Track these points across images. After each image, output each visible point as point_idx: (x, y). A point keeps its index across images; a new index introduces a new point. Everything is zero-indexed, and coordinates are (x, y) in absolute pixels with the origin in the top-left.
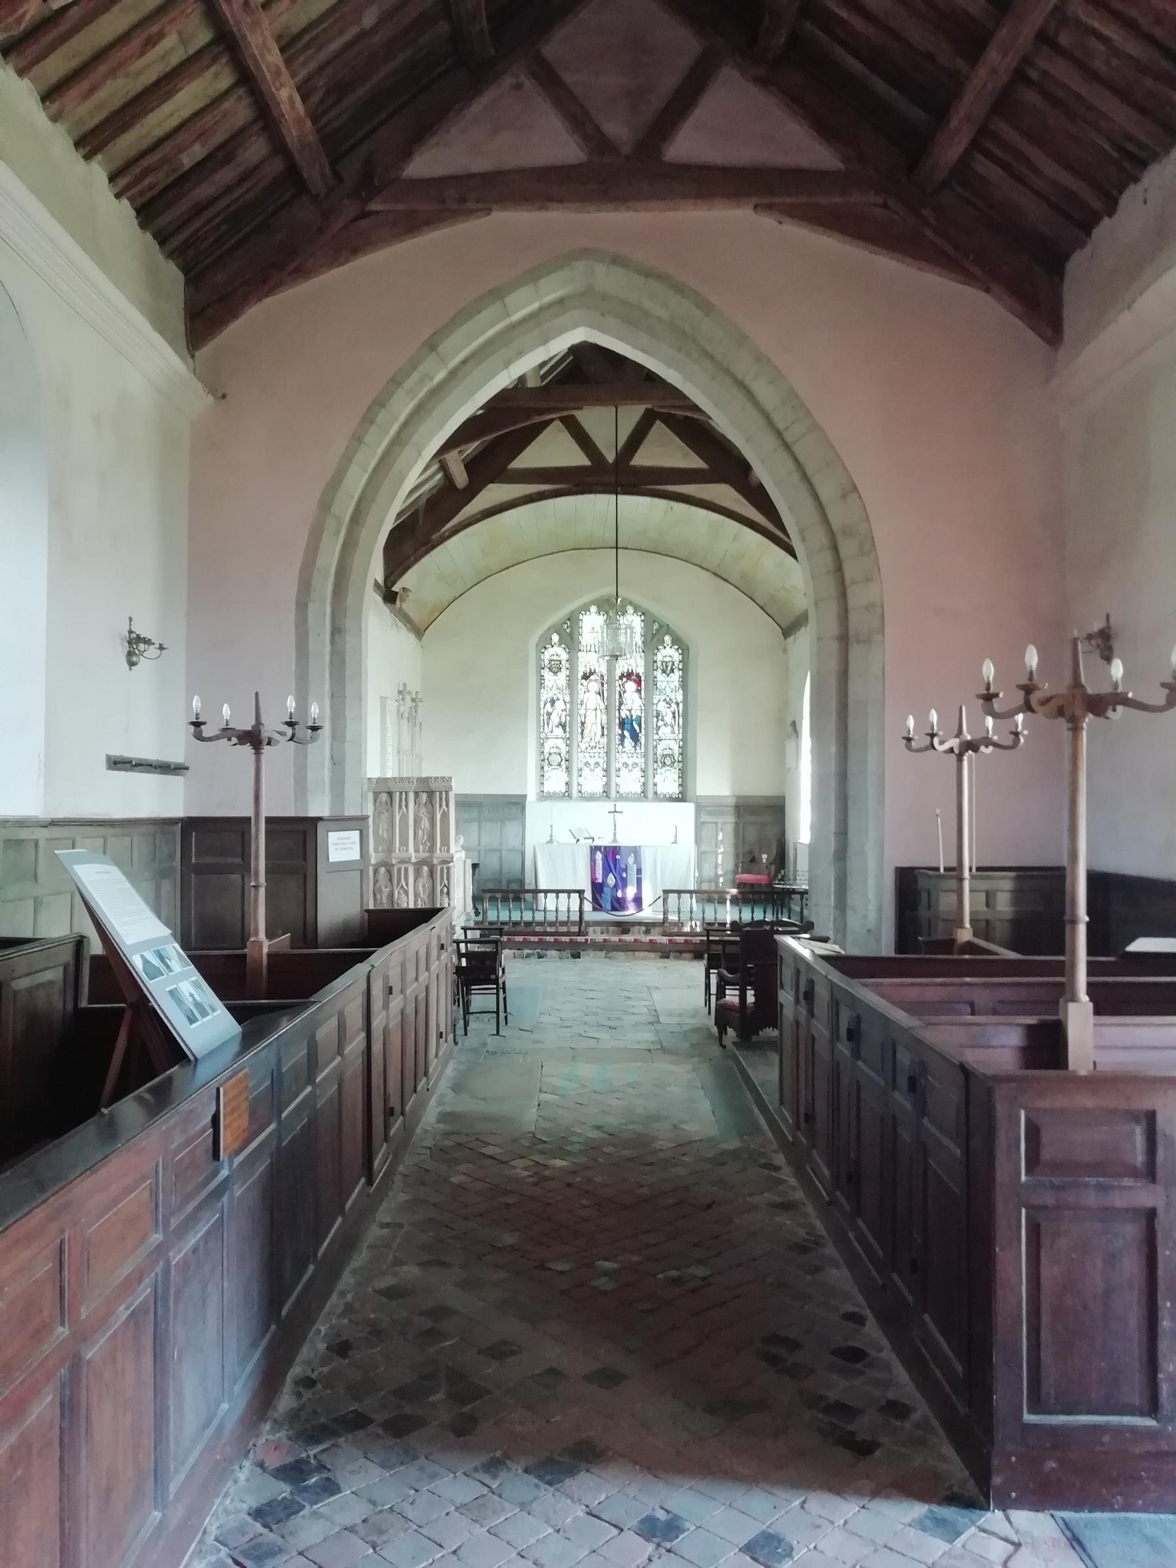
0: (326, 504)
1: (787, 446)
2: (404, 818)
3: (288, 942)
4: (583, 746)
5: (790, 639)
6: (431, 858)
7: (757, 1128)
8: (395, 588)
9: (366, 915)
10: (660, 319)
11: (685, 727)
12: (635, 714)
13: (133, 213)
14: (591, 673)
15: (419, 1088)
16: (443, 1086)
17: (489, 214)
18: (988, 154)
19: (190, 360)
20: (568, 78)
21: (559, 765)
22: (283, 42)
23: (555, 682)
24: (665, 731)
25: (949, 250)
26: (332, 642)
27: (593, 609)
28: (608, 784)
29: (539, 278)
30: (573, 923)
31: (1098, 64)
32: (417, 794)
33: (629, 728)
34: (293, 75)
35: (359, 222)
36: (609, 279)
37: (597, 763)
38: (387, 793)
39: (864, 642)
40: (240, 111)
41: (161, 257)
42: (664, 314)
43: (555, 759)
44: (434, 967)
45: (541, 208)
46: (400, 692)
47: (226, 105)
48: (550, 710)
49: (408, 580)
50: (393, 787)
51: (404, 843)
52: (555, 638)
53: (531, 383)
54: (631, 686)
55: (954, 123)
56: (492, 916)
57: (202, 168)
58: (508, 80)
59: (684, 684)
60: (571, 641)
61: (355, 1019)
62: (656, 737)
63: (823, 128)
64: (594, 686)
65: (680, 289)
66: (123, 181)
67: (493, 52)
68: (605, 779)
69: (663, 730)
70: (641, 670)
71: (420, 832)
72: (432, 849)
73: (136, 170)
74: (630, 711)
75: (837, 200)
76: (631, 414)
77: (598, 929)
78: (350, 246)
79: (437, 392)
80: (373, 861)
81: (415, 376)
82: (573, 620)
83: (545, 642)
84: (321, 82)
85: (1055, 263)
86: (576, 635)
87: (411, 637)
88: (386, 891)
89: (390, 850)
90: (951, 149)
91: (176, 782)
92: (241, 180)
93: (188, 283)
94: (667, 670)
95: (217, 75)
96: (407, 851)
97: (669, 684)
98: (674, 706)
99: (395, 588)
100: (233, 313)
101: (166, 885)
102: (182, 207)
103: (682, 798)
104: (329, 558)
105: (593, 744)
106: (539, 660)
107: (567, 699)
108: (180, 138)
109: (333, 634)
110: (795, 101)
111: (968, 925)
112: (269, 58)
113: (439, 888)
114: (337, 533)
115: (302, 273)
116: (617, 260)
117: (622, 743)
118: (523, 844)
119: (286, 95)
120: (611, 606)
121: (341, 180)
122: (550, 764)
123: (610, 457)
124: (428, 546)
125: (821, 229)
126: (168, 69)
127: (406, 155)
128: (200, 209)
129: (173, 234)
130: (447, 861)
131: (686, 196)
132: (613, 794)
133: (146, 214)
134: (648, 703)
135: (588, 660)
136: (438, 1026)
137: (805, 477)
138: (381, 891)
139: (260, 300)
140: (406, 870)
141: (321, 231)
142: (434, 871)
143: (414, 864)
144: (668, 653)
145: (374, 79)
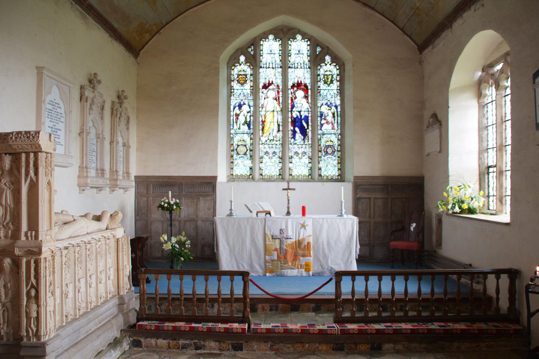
4: (263, 139)
6: (12, 246)
12: (303, 114)
14: (270, 84)
21: (245, 154)
23: (241, 92)
27: (271, 37)
28: (282, 169)
33: (299, 124)
37: (274, 152)
43: (242, 150)
48: (238, 112)
52: (242, 58)
54: (300, 94)
59: (341, 91)
60: (254, 61)
62: (320, 132)
64: (272, 94)
68: (281, 165)
69: (325, 127)
70: (308, 82)
72: (16, 235)
74: (300, 112)
82: (255, 43)
83: (233, 61)
86: (258, 56)
94: (328, 81)
97: (330, 93)
98: (333, 108)
103: (341, 178)
106: (229, 75)
107: (252, 103)
117: (294, 137)
118: (214, 215)
122: (238, 154)
132: (287, 176)
134: (314, 105)
135: (267, 75)
144: (329, 68)
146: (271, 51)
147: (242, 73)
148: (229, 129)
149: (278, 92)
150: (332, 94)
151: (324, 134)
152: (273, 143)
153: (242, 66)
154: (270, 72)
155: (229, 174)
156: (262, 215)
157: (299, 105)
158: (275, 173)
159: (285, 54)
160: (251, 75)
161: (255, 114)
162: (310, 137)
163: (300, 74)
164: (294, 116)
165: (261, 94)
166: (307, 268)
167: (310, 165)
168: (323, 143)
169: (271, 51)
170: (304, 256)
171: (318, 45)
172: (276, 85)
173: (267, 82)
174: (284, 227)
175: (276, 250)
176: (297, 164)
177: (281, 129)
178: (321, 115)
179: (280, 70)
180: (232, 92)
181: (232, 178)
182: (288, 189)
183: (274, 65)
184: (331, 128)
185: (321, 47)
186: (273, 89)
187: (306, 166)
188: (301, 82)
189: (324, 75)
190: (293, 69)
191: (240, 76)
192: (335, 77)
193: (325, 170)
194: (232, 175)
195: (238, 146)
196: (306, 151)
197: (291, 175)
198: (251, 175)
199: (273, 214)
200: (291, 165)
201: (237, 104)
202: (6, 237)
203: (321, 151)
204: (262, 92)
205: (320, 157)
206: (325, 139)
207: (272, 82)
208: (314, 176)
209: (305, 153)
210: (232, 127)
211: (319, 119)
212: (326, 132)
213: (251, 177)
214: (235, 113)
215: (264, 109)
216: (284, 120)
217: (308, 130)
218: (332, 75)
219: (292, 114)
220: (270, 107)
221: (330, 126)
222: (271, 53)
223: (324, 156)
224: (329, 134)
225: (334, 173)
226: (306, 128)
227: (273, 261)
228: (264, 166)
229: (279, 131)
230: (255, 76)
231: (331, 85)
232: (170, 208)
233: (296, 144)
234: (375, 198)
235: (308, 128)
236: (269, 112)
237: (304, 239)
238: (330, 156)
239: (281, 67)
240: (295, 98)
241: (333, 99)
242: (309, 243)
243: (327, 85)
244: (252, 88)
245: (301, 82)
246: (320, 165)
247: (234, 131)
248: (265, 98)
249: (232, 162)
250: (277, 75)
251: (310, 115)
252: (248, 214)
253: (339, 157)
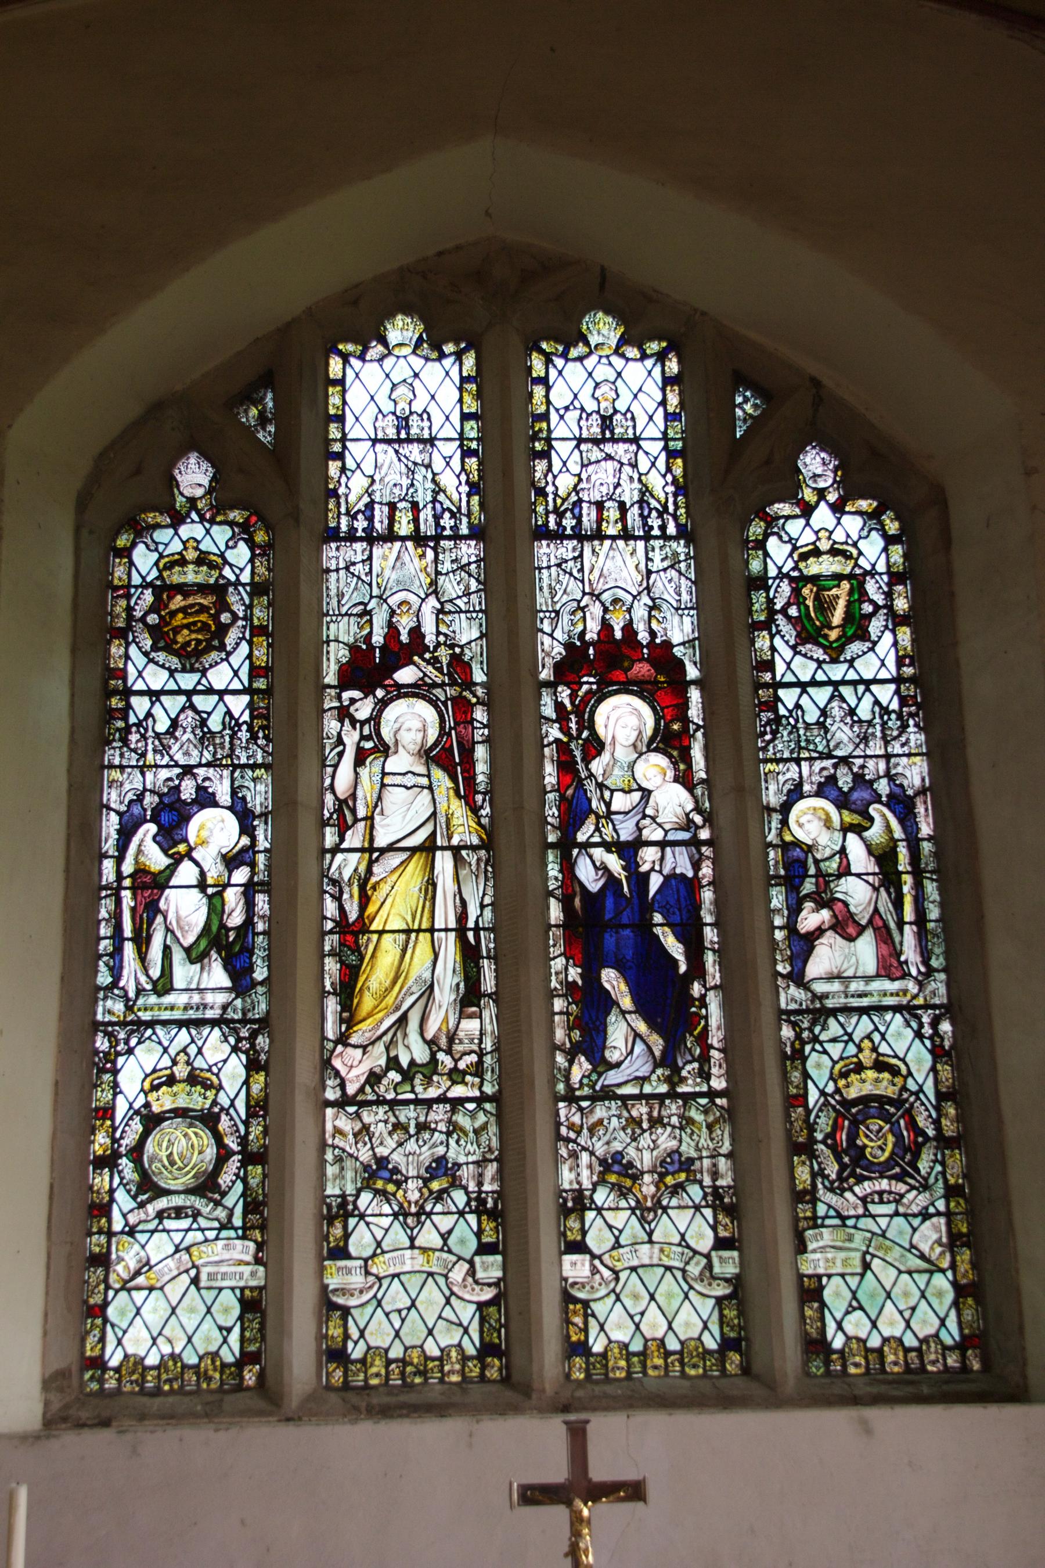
4: (354, 1066)
11: (961, 940)
21: (207, 1186)
27: (401, 330)
37: (440, 1167)
48: (156, 859)
52: (194, 476)
54: (623, 718)
59: (931, 690)
60: (284, 490)
62: (791, 996)
64: (411, 721)
68: (491, 1268)
69: (825, 958)
74: (628, 850)
83: (124, 497)
98: (883, 822)
105: (414, 1050)
107: (259, 794)
117: (591, 1043)
122: (148, 1187)
134: (730, 803)
144: (827, 531)
146: (403, 422)
147: (191, 575)
149: (463, 708)
150: (864, 711)
151: (821, 1013)
152: (433, 1093)
153: (192, 530)
154: (399, 567)
155: (67, 1359)
157: (620, 802)
158: (448, 1337)
159: (506, 436)
160: (257, 589)
162: (715, 1038)
163: (629, 581)
165: (332, 725)
167: (728, 1264)
169: (403, 422)
171: (740, 380)
172: (444, 654)
173: (378, 639)
176: (626, 1258)
177: (489, 983)
178: (792, 879)
179: (469, 551)
180: (110, 715)
183: (426, 515)
184: (869, 963)
185: (759, 391)
186: (419, 690)
187: (695, 1269)
188: (629, 629)
189: (798, 581)
190: (567, 549)
191: (178, 602)
193: (856, 1305)
194: (99, 1363)
195: (152, 1121)
196: (688, 1150)
197: (582, 1348)
198: (246, 1358)
200: (575, 1268)
201: (149, 800)
203: (807, 1149)
204: (344, 714)
205: (810, 1196)
206: (835, 1050)
207: (416, 633)
208: (765, 1355)
209: (687, 1165)
210: (104, 978)
211: (778, 898)
213: (242, 1387)
214: (128, 868)
215: (354, 838)
216: (513, 905)
217: (696, 989)
218: (858, 581)
219: (568, 867)
220: (401, 817)
221: (865, 952)
222: (404, 433)
223: (839, 1187)
225: (926, 1323)
226: (683, 968)
228: (357, 1280)
229: (470, 997)
230: (289, 599)
231: (855, 648)
233: (607, 1094)
235: (697, 970)
236: (395, 860)
238: (884, 1184)
239: (477, 533)
240: (595, 746)
241: (876, 747)
243: (819, 654)
244: (261, 684)
245: (629, 629)
246: (813, 1263)
247: (119, 1007)
248: (361, 758)
249: (102, 1260)
250: (451, 587)
251: (706, 870)
253: (951, 1192)
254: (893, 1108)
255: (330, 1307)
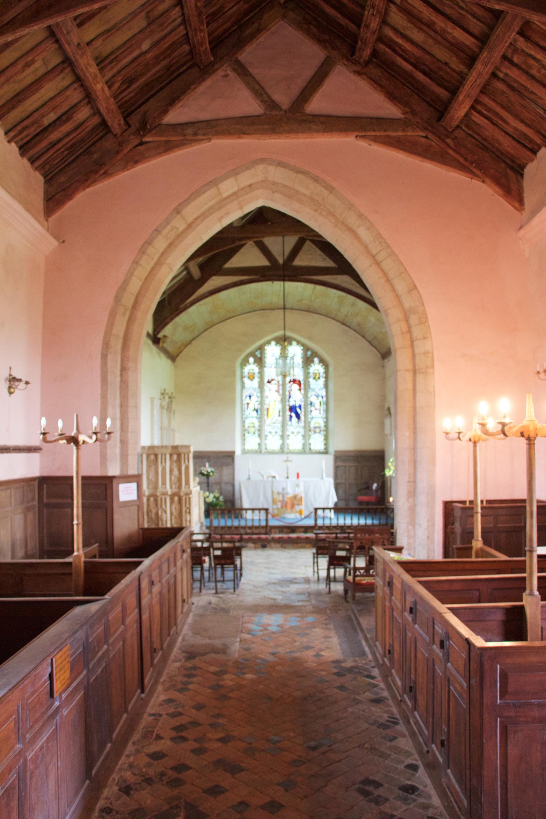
0: (118, 299)
1: (378, 264)
2: (164, 469)
3: (97, 550)
5: (386, 360)
6: (180, 491)
7: (363, 654)
8: (160, 336)
9: (141, 531)
10: (305, 195)
13: (17, 149)
15: (172, 633)
16: (186, 630)
17: (210, 142)
18: (479, 112)
19: (46, 223)
20: (252, 71)
22: (99, 60)
23: (251, 385)
24: (315, 413)
25: (462, 160)
26: (121, 375)
27: (273, 343)
28: (283, 445)
29: (237, 174)
30: (263, 527)
31: (534, 72)
32: (171, 455)
34: (103, 77)
35: (139, 147)
36: (276, 174)
37: (276, 432)
38: (153, 454)
39: (423, 373)
40: (76, 96)
41: (32, 170)
42: (307, 193)
43: (252, 430)
44: (179, 563)
45: (239, 138)
46: (162, 394)
47: (68, 93)
49: (167, 331)
50: (157, 451)
51: (164, 483)
52: (251, 360)
53: (236, 225)
54: (295, 387)
55: (461, 98)
56: (215, 523)
57: (54, 124)
58: (221, 73)
59: (326, 386)
60: (260, 361)
61: (132, 600)
63: (391, 96)
64: (273, 386)
65: (316, 179)
66: (12, 134)
67: (212, 59)
71: (173, 478)
72: (180, 487)
73: (19, 128)
75: (400, 134)
76: (291, 241)
77: (277, 530)
78: (134, 160)
79: (181, 236)
80: (147, 493)
81: (169, 227)
82: (261, 348)
83: (245, 362)
84: (120, 78)
85: (519, 170)
86: (263, 358)
87: (169, 362)
88: (154, 511)
89: (156, 487)
90: (460, 110)
91: (35, 456)
92: (75, 129)
93: (46, 182)
95: (63, 78)
96: (165, 488)
97: (317, 386)
98: (320, 399)
99: (160, 336)
100: (69, 197)
101: (30, 516)
102: (44, 144)
103: (326, 452)
104: (119, 329)
105: (274, 421)
106: (242, 373)
107: (259, 395)
108: (42, 111)
109: (121, 371)
110: (376, 83)
111: (480, 539)
112: (91, 70)
113: (184, 509)
114: (124, 314)
115: (107, 174)
116: (281, 164)
119: (99, 87)
120: (284, 341)
121: (129, 126)
123: (281, 261)
124: (177, 311)
125: (392, 149)
126: (37, 77)
127: (165, 112)
128: (53, 145)
129: (38, 158)
130: (188, 494)
131: (318, 131)
133: (23, 149)
134: (306, 396)
135: (270, 372)
136: (182, 596)
137: (388, 280)
138: (151, 511)
139: (84, 189)
140: (165, 499)
141: (118, 153)
142: (181, 500)
143: (170, 496)
144: (317, 368)
145: (149, 75)
147: (251, 371)
148: (242, 415)
151: (313, 418)
156: (270, 479)
159: (284, 355)
161: (262, 403)
164: (291, 405)
166: (300, 512)
168: (312, 425)
170: (298, 505)
174: (285, 486)
175: (280, 501)
178: (311, 404)
181: (244, 452)
182: (287, 461)
192: (321, 374)
199: (277, 478)
202: (175, 488)
208: (306, 450)
212: (314, 416)
213: (259, 452)
221: (318, 411)
224: (317, 417)
227: (278, 509)
229: (279, 415)
230: (261, 373)
231: (319, 380)
232: (208, 476)
234: (350, 466)
237: (298, 494)
242: (301, 498)
252: (261, 478)
254: (319, 427)
255: (266, 445)
